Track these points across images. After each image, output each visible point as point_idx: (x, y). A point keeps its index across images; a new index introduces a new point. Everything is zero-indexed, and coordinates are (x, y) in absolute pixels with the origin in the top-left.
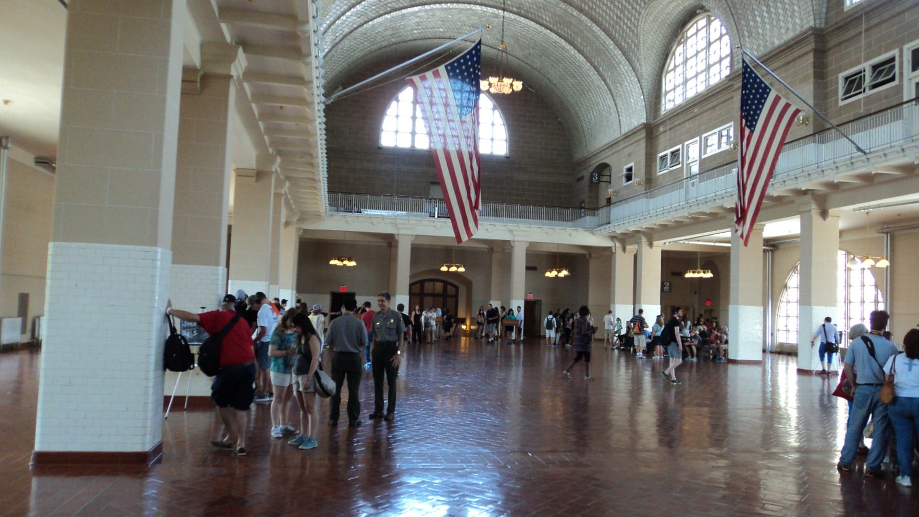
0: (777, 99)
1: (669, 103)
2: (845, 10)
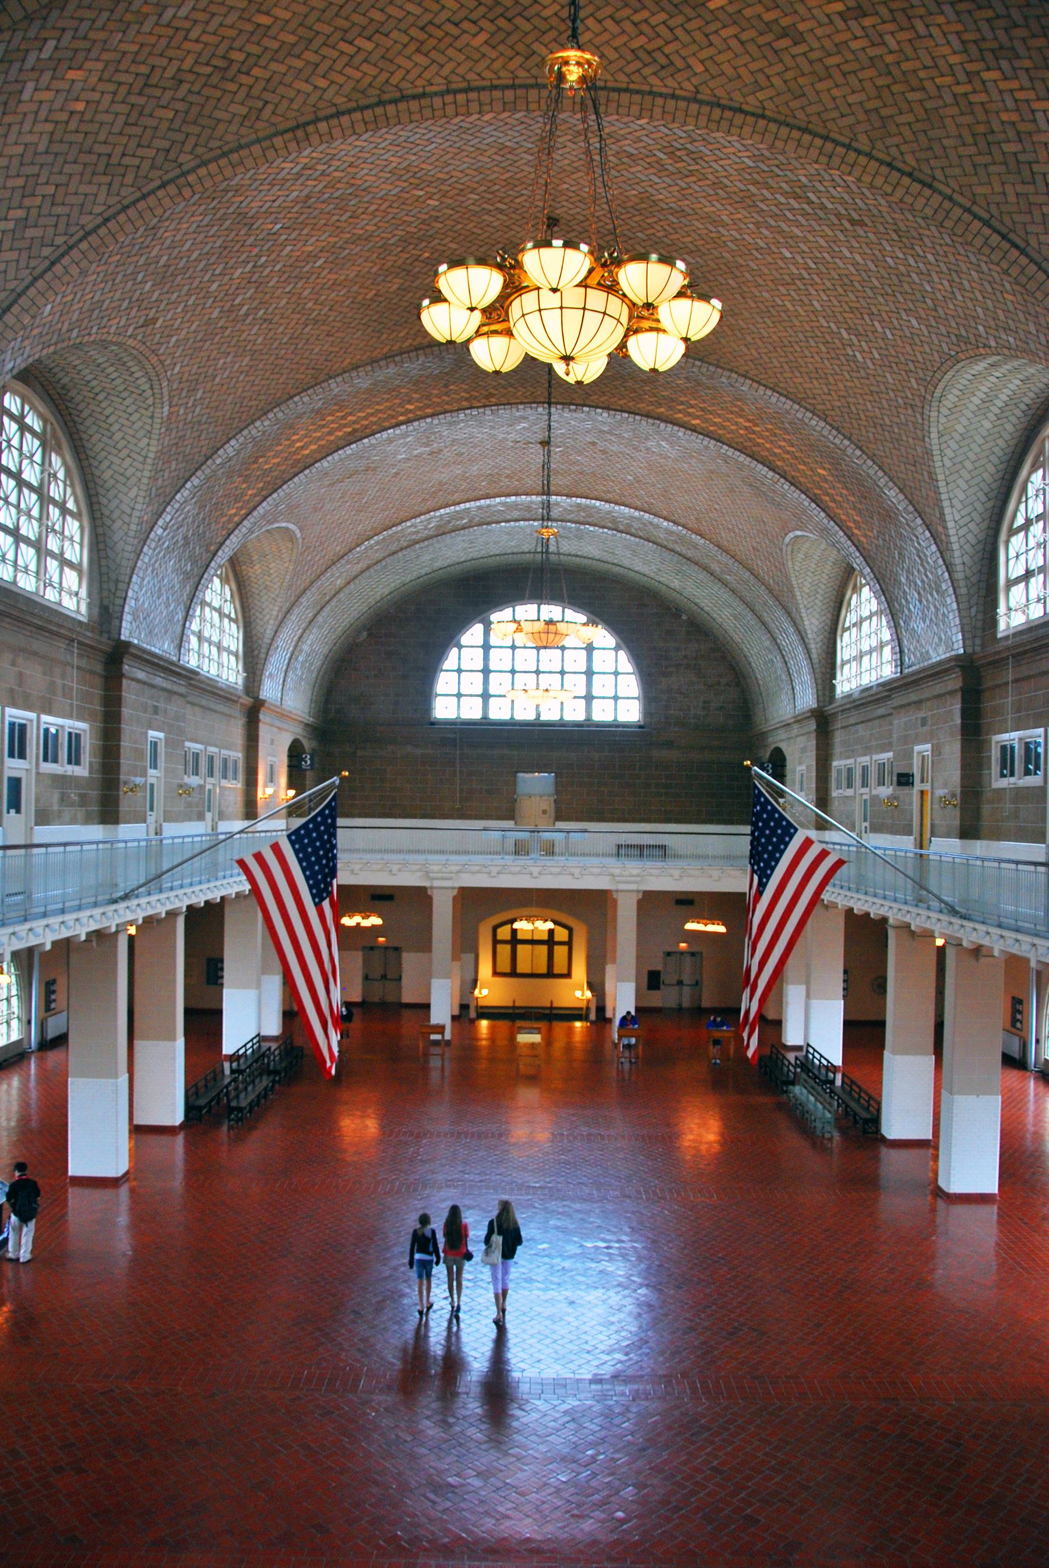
1: (849, 681)
2: (999, 636)
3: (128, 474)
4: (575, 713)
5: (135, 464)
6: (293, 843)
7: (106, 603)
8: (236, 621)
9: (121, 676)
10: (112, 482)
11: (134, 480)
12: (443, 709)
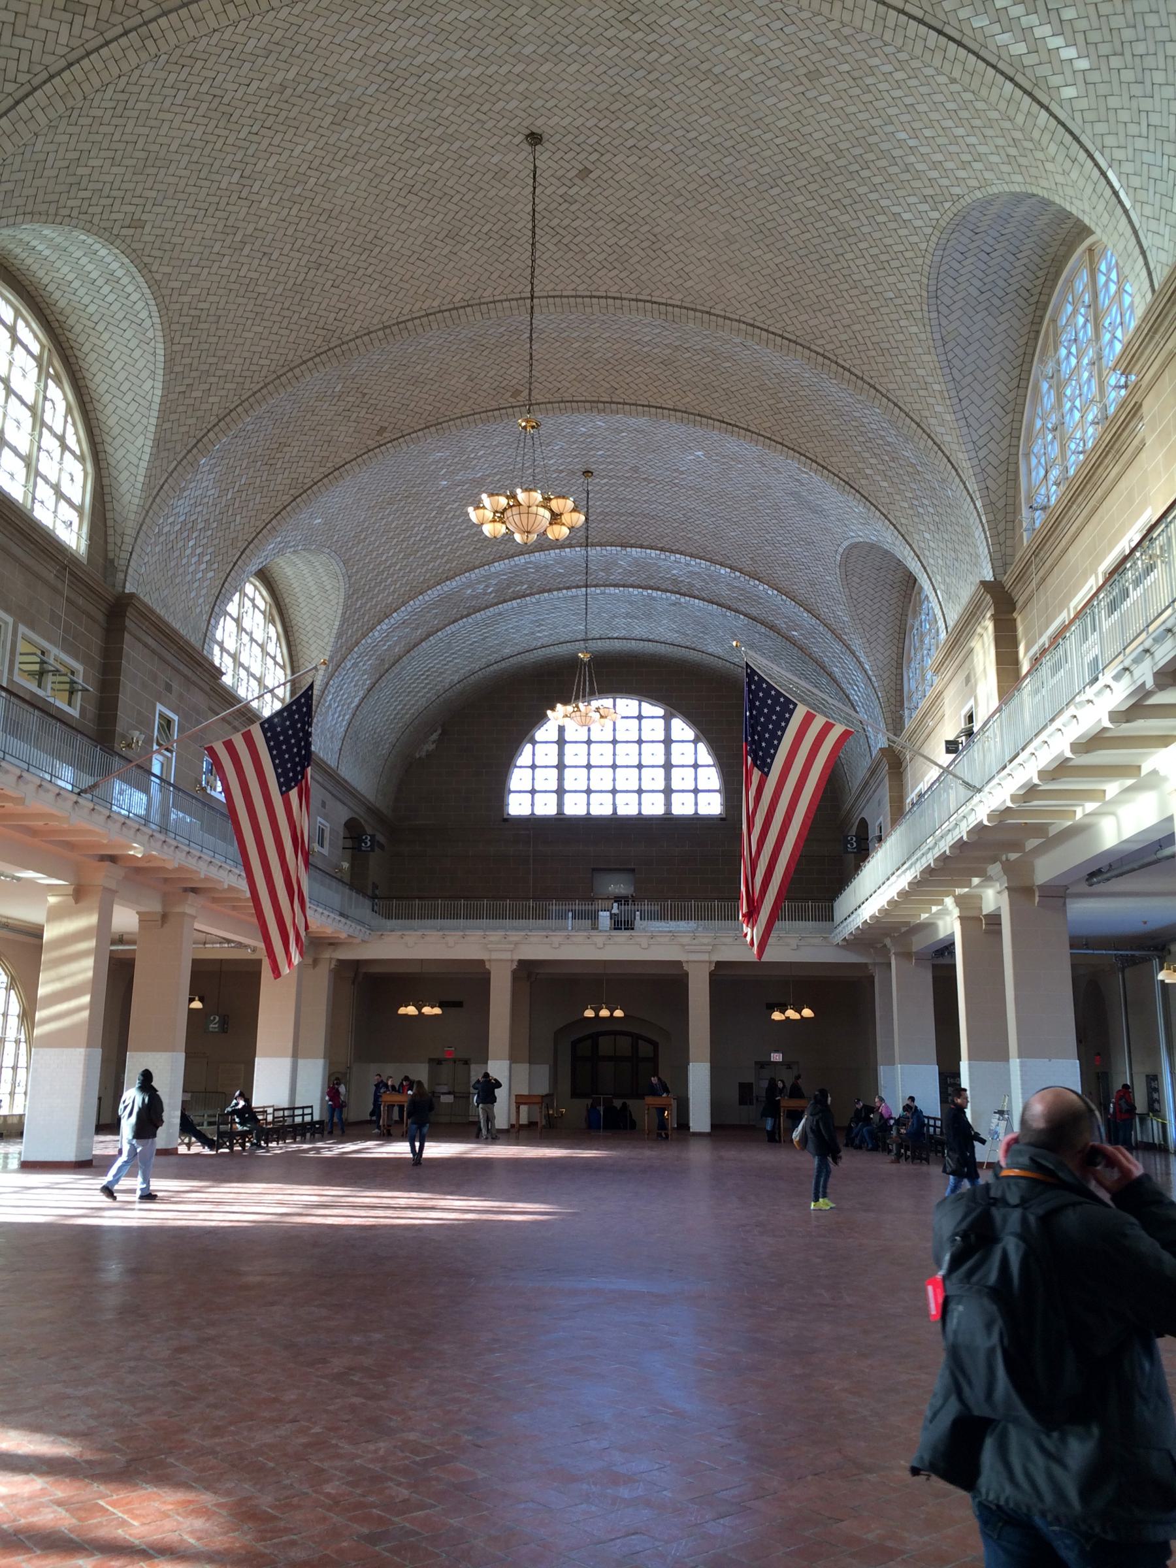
0: (808, 719)
3: (134, 420)
4: (654, 807)
5: (141, 409)
6: (265, 731)
7: (111, 555)
8: (283, 667)
9: (123, 629)
10: (117, 430)
11: (140, 428)
12: (517, 806)
